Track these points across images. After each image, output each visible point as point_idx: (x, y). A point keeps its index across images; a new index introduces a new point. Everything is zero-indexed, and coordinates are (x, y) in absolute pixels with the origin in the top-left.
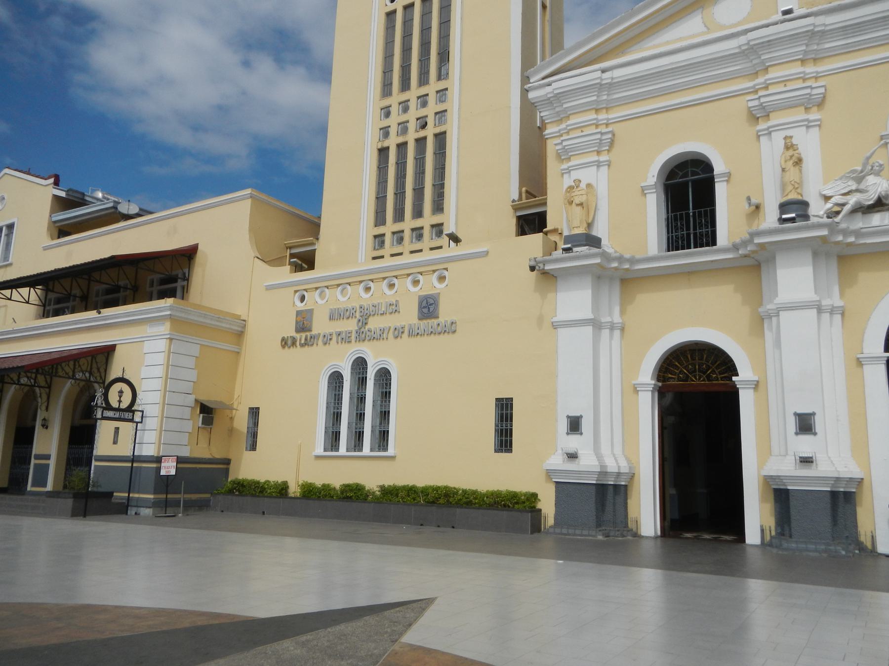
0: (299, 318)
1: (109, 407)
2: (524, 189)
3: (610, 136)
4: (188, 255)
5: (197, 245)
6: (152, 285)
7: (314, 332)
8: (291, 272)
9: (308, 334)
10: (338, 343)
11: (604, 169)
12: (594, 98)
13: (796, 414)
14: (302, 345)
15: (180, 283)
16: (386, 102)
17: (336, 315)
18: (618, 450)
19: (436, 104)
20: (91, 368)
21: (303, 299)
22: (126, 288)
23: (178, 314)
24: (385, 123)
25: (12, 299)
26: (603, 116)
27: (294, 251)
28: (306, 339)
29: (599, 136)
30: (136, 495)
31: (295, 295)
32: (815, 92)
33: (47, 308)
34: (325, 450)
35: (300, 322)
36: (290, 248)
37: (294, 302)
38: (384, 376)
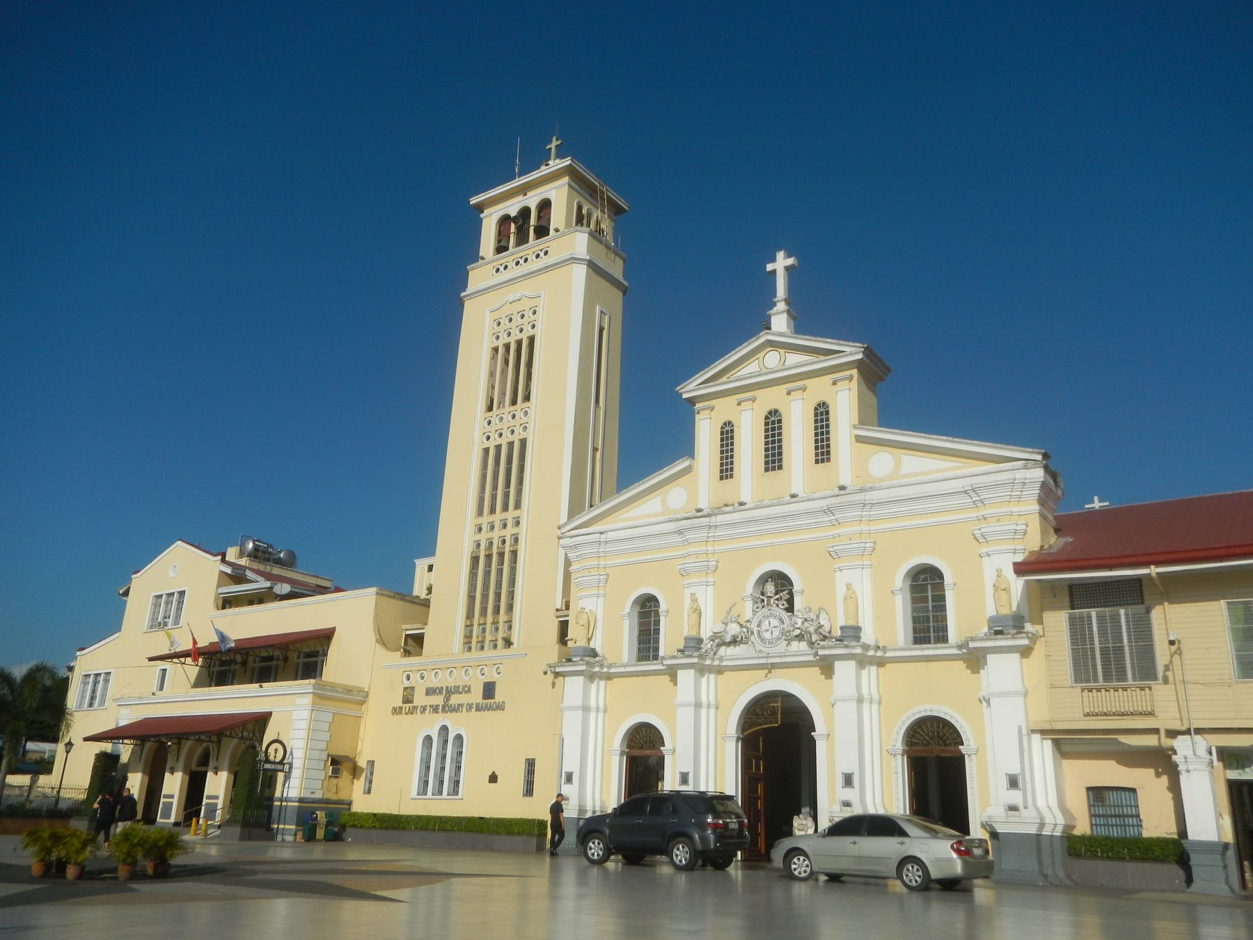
0: (405, 693)
1: (267, 761)
2: (564, 601)
3: (604, 577)
4: (326, 636)
6: (299, 658)
9: (411, 705)
11: (601, 599)
12: (597, 550)
13: (680, 772)
14: (406, 714)
15: (319, 659)
17: (430, 692)
18: (597, 796)
20: (254, 730)
21: (408, 678)
22: (278, 659)
24: (478, 537)
26: (602, 563)
27: (408, 632)
29: (598, 577)
32: (710, 564)
33: (212, 669)
34: (418, 794)
36: (407, 630)
38: (459, 738)
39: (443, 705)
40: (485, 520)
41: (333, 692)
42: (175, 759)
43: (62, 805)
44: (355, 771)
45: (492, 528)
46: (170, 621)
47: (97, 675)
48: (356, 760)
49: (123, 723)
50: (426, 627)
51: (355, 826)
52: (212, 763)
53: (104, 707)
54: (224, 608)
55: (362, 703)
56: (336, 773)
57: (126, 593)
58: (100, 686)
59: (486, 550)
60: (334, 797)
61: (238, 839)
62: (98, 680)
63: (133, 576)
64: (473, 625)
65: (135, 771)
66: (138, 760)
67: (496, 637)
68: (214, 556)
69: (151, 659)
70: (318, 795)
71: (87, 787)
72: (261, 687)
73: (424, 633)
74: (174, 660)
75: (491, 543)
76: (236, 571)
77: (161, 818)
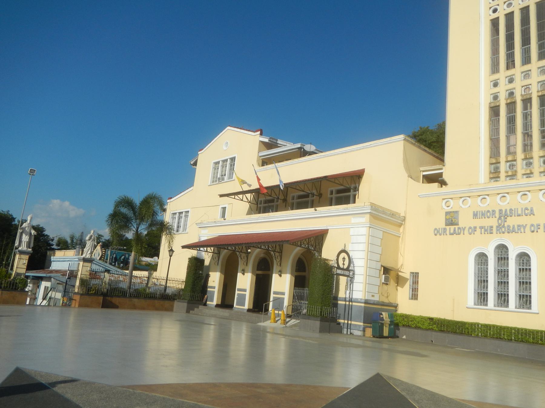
1: (339, 268)
5: (364, 169)
6: (332, 193)
7: (461, 225)
8: (438, 187)
9: (456, 227)
10: (481, 234)
14: (451, 234)
15: (352, 193)
16: (495, 77)
19: (538, 76)
23: (374, 212)
24: (495, 90)
25: (243, 200)
28: (455, 230)
30: (353, 323)
31: (442, 202)
33: (259, 206)
35: (449, 219)
37: (442, 206)
39: (497, 227)
40: (503, 74)
41: (383, 214)
42: (245, 264)
43: (169, 291)
44: (399, 281)
45: (511, 81)
46: (226, 178)
47: (181, 213)
48: (399, 270)
49: (203, 239)
50: (444, 168)
51: (409, 326)
52: (276, 267)
53: (186, 232)
54: (263, 165)
55: (400, 225)
56: (387, 279)
57: (195, 164)
58: (183, 220)
59: (506, 99)
60: (386, 301)
61: (318, 330)
62: (182, 215)
63: (199, 153)
64: (499, 163)
65: (215, 271)
66: (216, 264)
67: (531, 171)
68: (254, 132)
69: (221, 196)
70: (376, 298)
71: (185, 280)
72: (316, 210)
73: (442, 173)
74: (236, 197)
75: (511, 94)
76: (271, 140)
77: (237, 305)
